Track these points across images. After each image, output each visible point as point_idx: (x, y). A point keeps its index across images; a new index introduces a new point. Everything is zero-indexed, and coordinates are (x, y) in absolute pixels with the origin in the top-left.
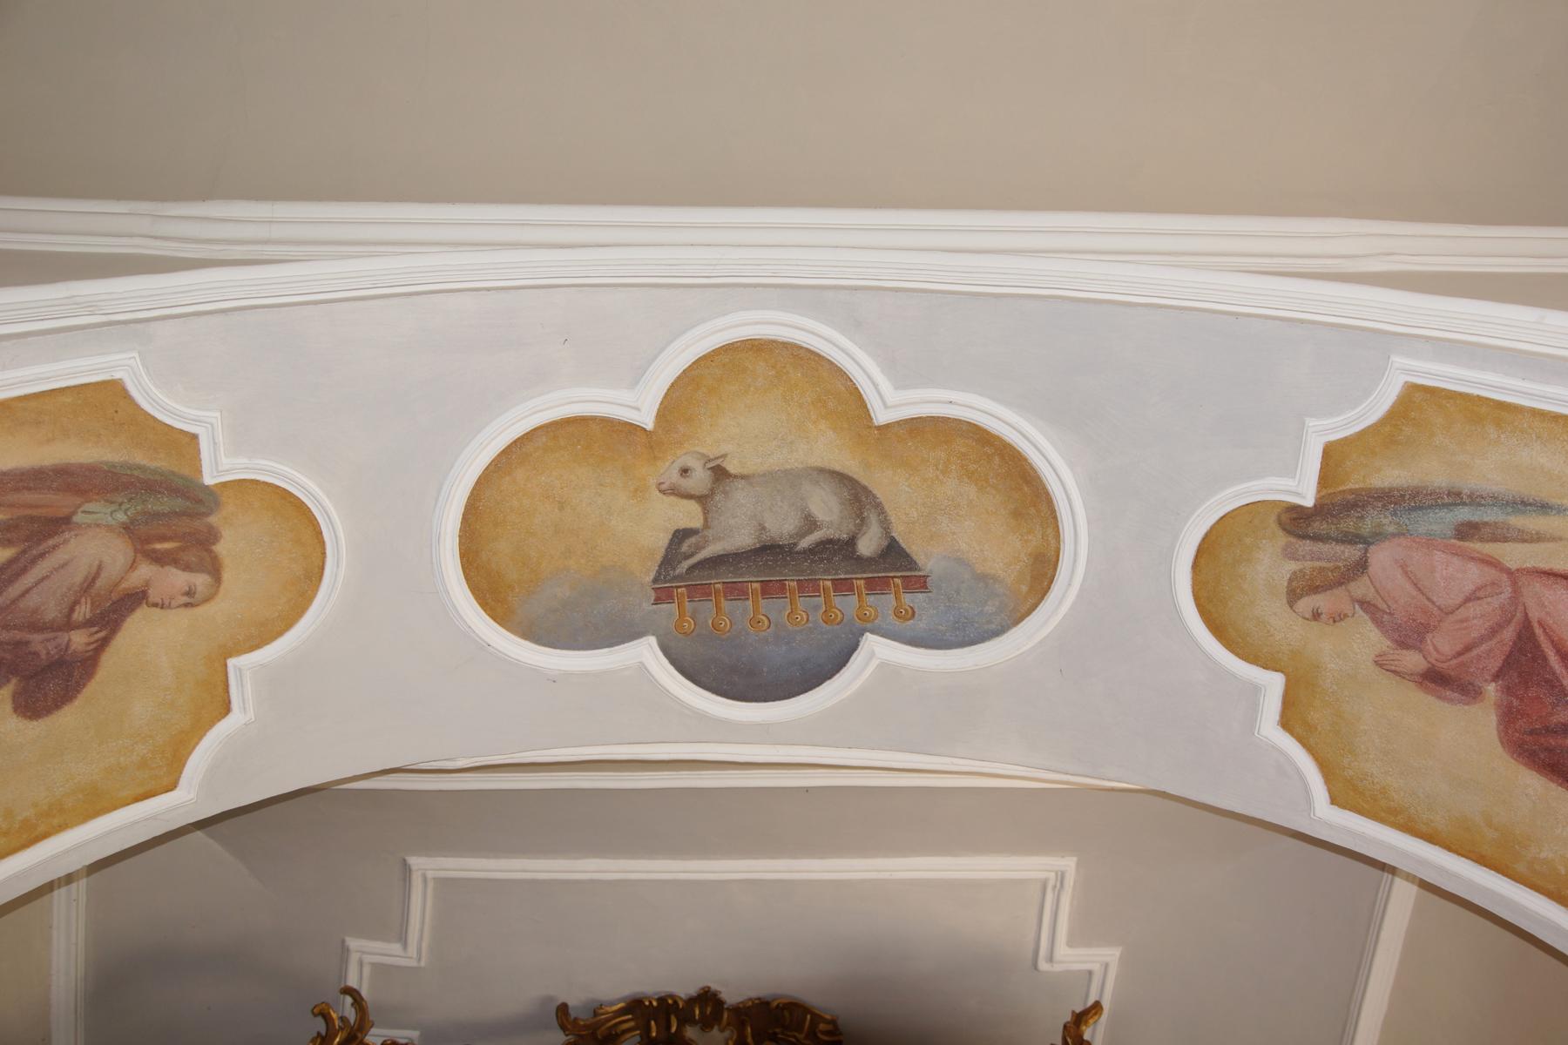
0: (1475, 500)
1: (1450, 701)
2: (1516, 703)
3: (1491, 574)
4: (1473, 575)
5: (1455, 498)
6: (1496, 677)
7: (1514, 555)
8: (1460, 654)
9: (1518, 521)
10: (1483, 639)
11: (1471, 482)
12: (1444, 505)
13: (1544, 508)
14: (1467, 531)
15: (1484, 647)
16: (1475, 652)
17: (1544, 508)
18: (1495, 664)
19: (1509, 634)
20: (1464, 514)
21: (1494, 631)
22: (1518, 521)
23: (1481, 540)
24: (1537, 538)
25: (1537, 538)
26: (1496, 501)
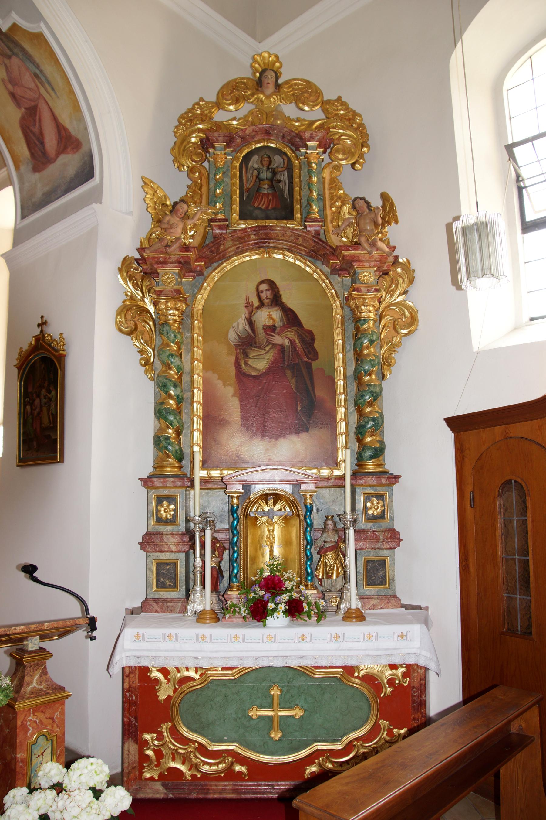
0: (41, 72)
1: (14, 103)
2: (26, 117)
3: (36, 89)
4: (32, 85)
5: (38, 67)
6: (26, 109)
7: (43, 91)
8: (21, 96)
9: (46, 84)
10: (27, 99)
11: (42, 67)
12: (35, 66)
13: (53, 89)
14: (36, 76)
15: (26, 101)
16: (24, 99)
17: (53, 89)
18: (27, 106)
19: (33, 104)
20: (38, 72)
21: (30, 100)
22: (46, 84)
23: (38, 81)
24: (48, 93)
25: (48, 93)
26: (45, 77)
